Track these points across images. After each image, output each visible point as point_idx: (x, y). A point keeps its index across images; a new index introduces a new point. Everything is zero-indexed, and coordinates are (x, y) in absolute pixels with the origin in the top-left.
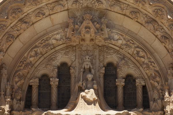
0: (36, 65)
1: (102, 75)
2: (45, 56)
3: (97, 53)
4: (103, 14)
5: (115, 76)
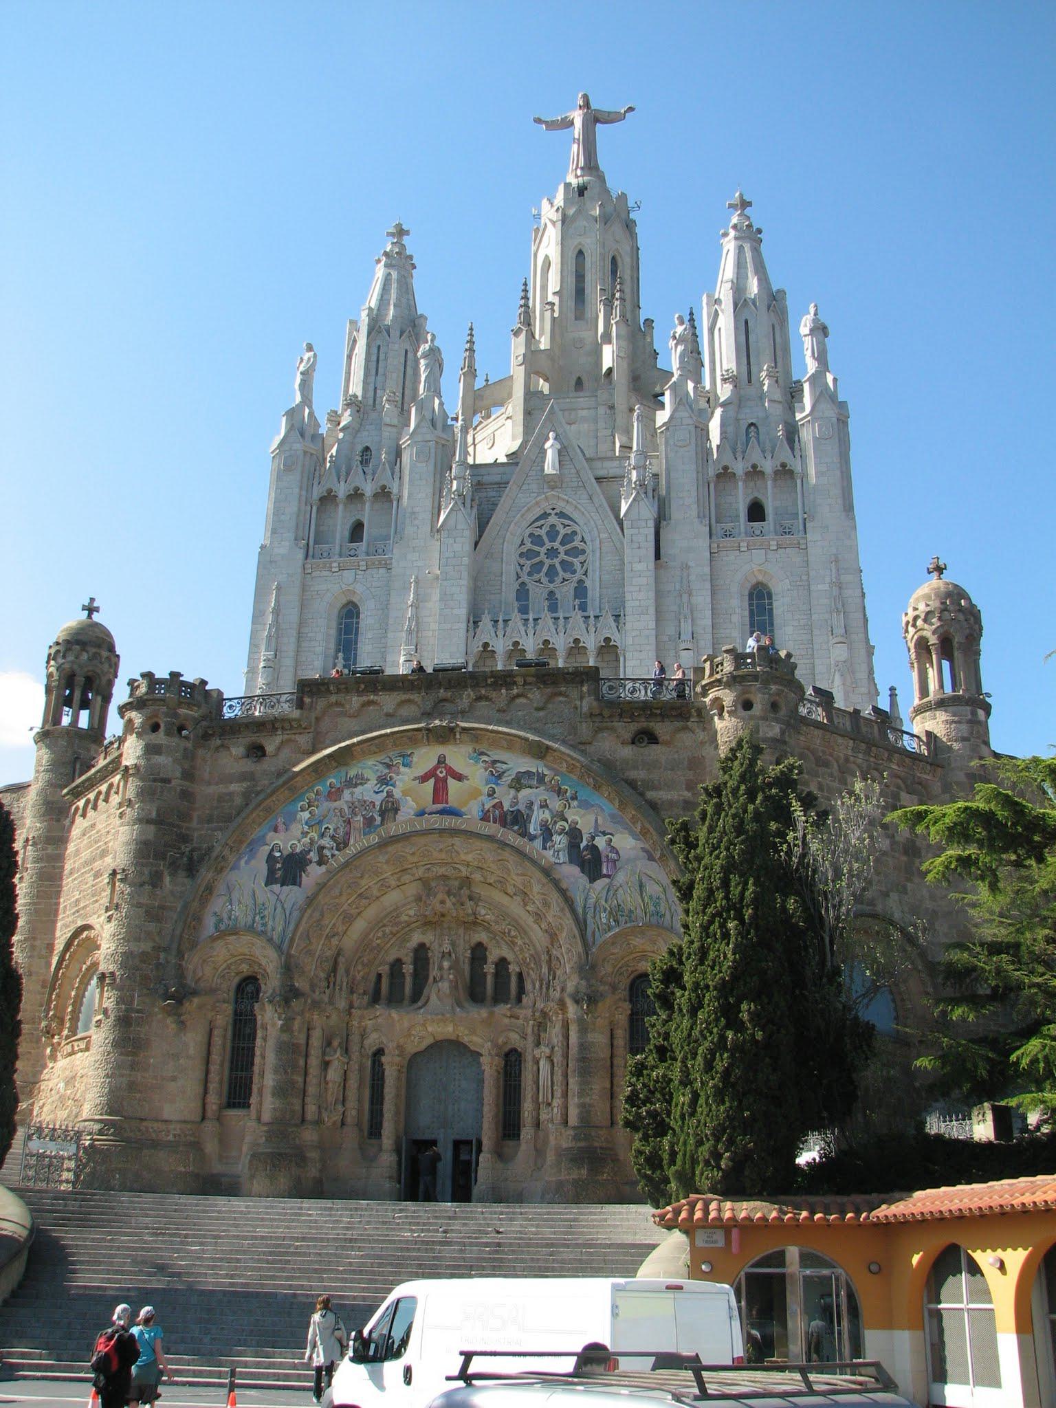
0: (386, 948)
1: (467, 960)
2: (398, 935)
3: (461, 931)
4: (467, 882)
5: (484, 960)
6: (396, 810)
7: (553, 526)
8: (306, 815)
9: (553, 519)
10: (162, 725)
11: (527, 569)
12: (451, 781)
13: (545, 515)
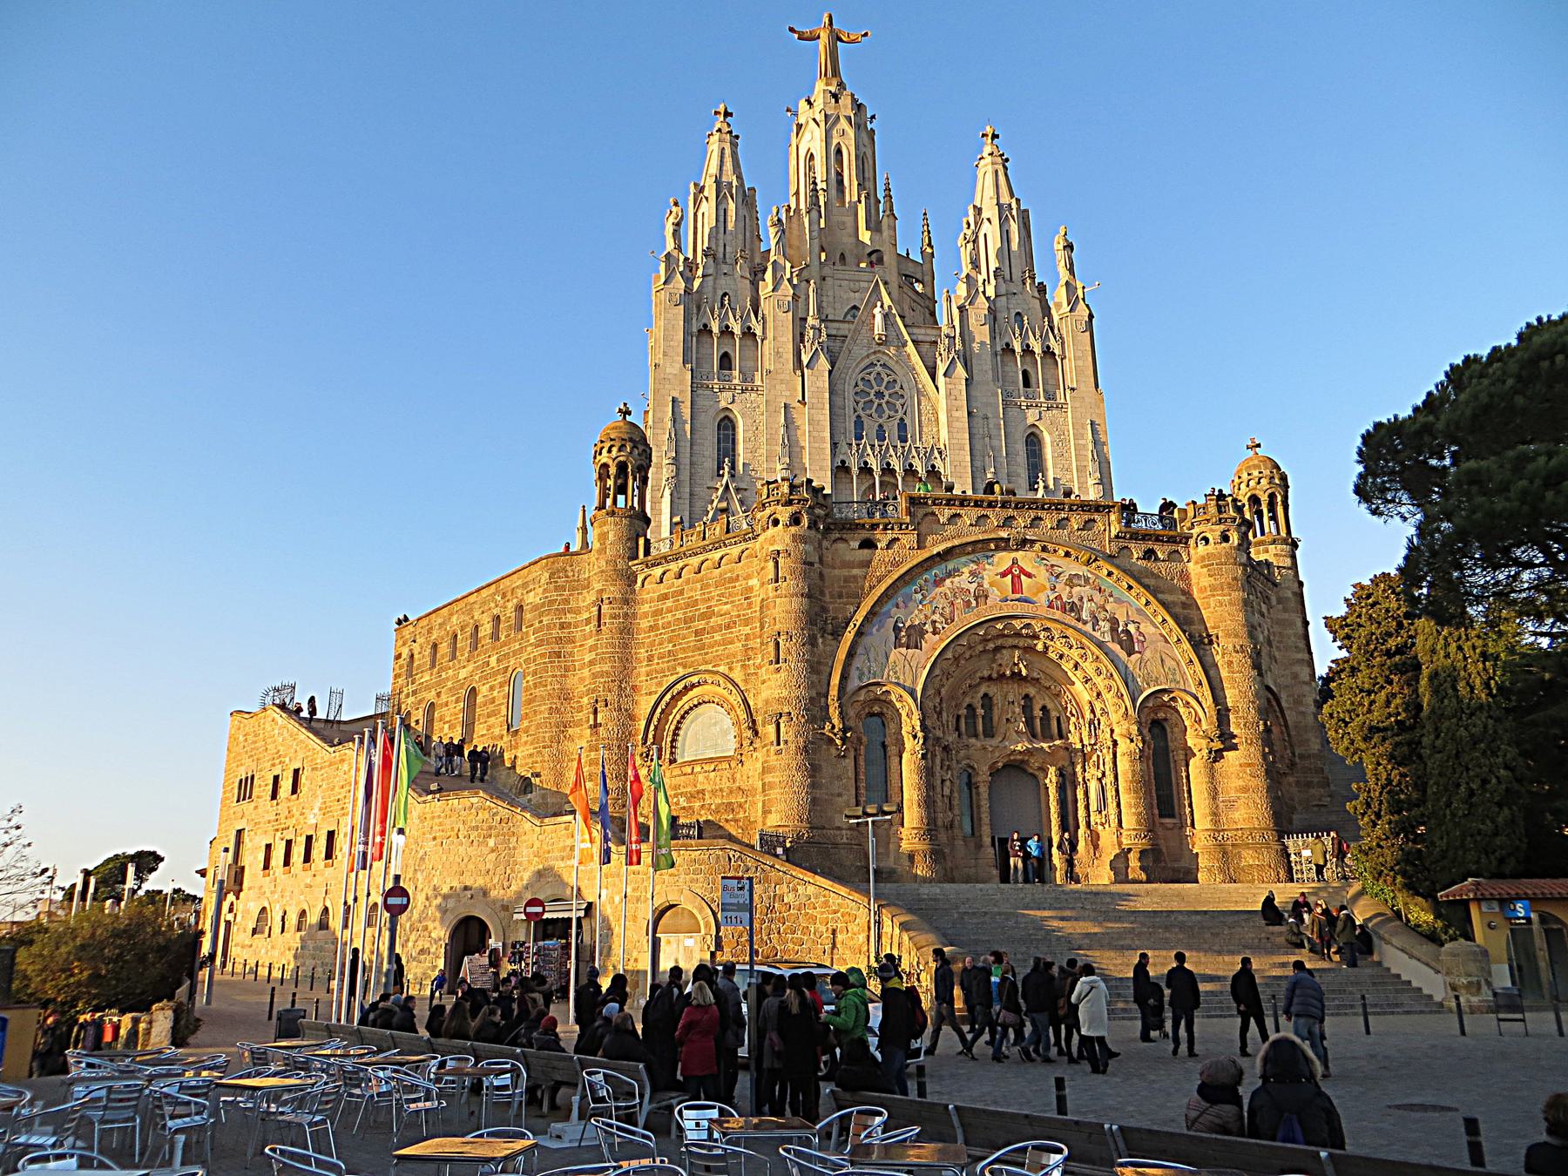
6: (986, 597)
7: (879, 374)
8: (919, 596)
9: (878, 368)
10: (805, 521)
11: (861, 405)
12: (1023, 577)
13: (872, 365)
